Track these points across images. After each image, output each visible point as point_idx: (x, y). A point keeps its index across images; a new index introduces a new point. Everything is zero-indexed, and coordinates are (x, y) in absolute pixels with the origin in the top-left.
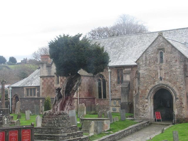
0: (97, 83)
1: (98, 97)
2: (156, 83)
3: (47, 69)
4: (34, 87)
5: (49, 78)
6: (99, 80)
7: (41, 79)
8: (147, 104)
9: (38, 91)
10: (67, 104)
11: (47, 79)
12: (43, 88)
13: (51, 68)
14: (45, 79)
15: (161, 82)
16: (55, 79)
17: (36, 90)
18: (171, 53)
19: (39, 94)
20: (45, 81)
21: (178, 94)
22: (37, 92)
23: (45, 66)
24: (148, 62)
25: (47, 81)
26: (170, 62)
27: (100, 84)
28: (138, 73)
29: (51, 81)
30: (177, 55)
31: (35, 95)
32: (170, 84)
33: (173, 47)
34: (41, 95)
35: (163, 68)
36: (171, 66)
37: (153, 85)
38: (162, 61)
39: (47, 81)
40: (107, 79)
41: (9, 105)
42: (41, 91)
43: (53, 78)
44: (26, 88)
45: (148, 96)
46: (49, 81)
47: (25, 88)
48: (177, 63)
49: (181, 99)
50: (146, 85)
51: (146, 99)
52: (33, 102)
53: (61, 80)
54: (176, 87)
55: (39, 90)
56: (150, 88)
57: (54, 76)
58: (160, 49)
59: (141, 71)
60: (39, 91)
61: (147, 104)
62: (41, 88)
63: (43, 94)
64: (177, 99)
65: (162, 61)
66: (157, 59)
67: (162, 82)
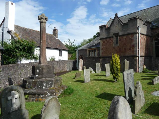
1: (155, 56)
3: (106, 32)
4: (95, 49)
5: (108, 40)
7: (101, 41)
9: (98, 52)
11: (106, 40)
12: (102, 49)
14: (104, 40)
16: (114, 40)
17: (97, 51)
20: (104, 42)
25: (106, 42)
34: (101, 55)
39: (106, 42)
41: (77, 63)
42: (101, 51)
43: (112, 39)
44: (89, 50)
46: (108, 42)
47: (87, 50)
52: (94, 60)
53: (120, 40)
55: (99, 50)
57: (112, 37)
60: (99, 52)
63: (102, 53)
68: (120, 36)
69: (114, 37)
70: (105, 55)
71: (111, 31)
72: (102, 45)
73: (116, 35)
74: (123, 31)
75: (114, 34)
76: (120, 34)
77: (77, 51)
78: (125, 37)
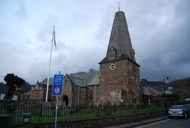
32: (67, 94)
36: (68, 87)
58: (65, 80)
65: (66, 85)
67: (65, 93)
74: (38, 89)
78: (39, 91)
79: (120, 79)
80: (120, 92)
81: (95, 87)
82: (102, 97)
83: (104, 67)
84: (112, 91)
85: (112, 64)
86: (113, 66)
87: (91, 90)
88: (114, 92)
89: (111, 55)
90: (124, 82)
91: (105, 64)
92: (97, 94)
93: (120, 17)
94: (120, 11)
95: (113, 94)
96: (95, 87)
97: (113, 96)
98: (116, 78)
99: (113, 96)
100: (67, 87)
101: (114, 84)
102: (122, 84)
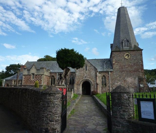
0: (51, 79)
2: (84, 79)
5: (28, 76)
6: (52, 78)
8: (79, 88)
10: (63, 82)
12: (24, 81)
13: (30, 71)
14: (26, 76)
15: (86, 78)
17: (20, 81)
18: (90, 67)
19: (21, 83)
20: (26, 77)
21: (93, 83)
22: (20, 82)
23: (26, 70)
24: (80, 70)
26: (90, 70)
27: (52, 80)
28: (76, 75)
29: (30, 77)
30: (93, 68)
31: (19, 84)
32: (90, 79)
33: (91, 64)
34: (23, 84)
35: (87, 72)
36: (90, 72)
37: (82, 80)
38: (86, 70)
40: (56, 78)
42: (23, 82)
43: (30, 76)
45: (80, 83)
48: (93, 71)
49: (94, 85)
50: (79, 79)
51: (79, 85)
53: (35, 77)
54: (92, 80)
56: (81, 81)
57: (31, 75)
59: (76, 74)
61: (79, 88)
62: (23, 80)
63: (24, 83)
64: (92, 85)
65: (86, 70)
66: (84, 69)
67: (86, 78)
68: (35, 75)
69: (32, 75)
70: (25, 84)
71: (30, 71)
72: (24, 78)
73: (33, 74)
74: (37, 72)
75: (32, 74)
76: (35, 74)
77: (4, 80)
79: (135, 67)
80: (137, 78)
81: (110, 73)
82: (117, 83)
83: (118, 56)
84: (128, 77)
85: (126, 53)
86: (127, 55)
87: (104, 76)
88: (130, 78)
89: (125, 46)
90: (140, 70)
91: (119, 53)
92: (112, 80)
93: (122, 13)
94: (123, 6)
95: (130, 80)
96: (110, 73)
97: (130, 82)
98: (131, 66)
99: (130, 82)
100: (87, 71)
101: (130, 72)
102: (138, 71)
